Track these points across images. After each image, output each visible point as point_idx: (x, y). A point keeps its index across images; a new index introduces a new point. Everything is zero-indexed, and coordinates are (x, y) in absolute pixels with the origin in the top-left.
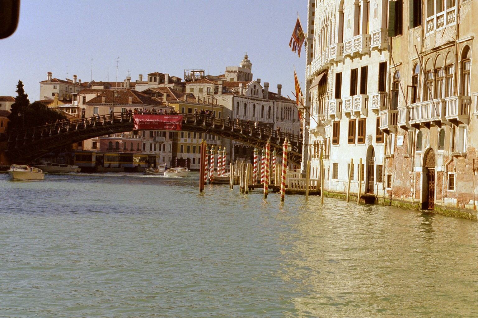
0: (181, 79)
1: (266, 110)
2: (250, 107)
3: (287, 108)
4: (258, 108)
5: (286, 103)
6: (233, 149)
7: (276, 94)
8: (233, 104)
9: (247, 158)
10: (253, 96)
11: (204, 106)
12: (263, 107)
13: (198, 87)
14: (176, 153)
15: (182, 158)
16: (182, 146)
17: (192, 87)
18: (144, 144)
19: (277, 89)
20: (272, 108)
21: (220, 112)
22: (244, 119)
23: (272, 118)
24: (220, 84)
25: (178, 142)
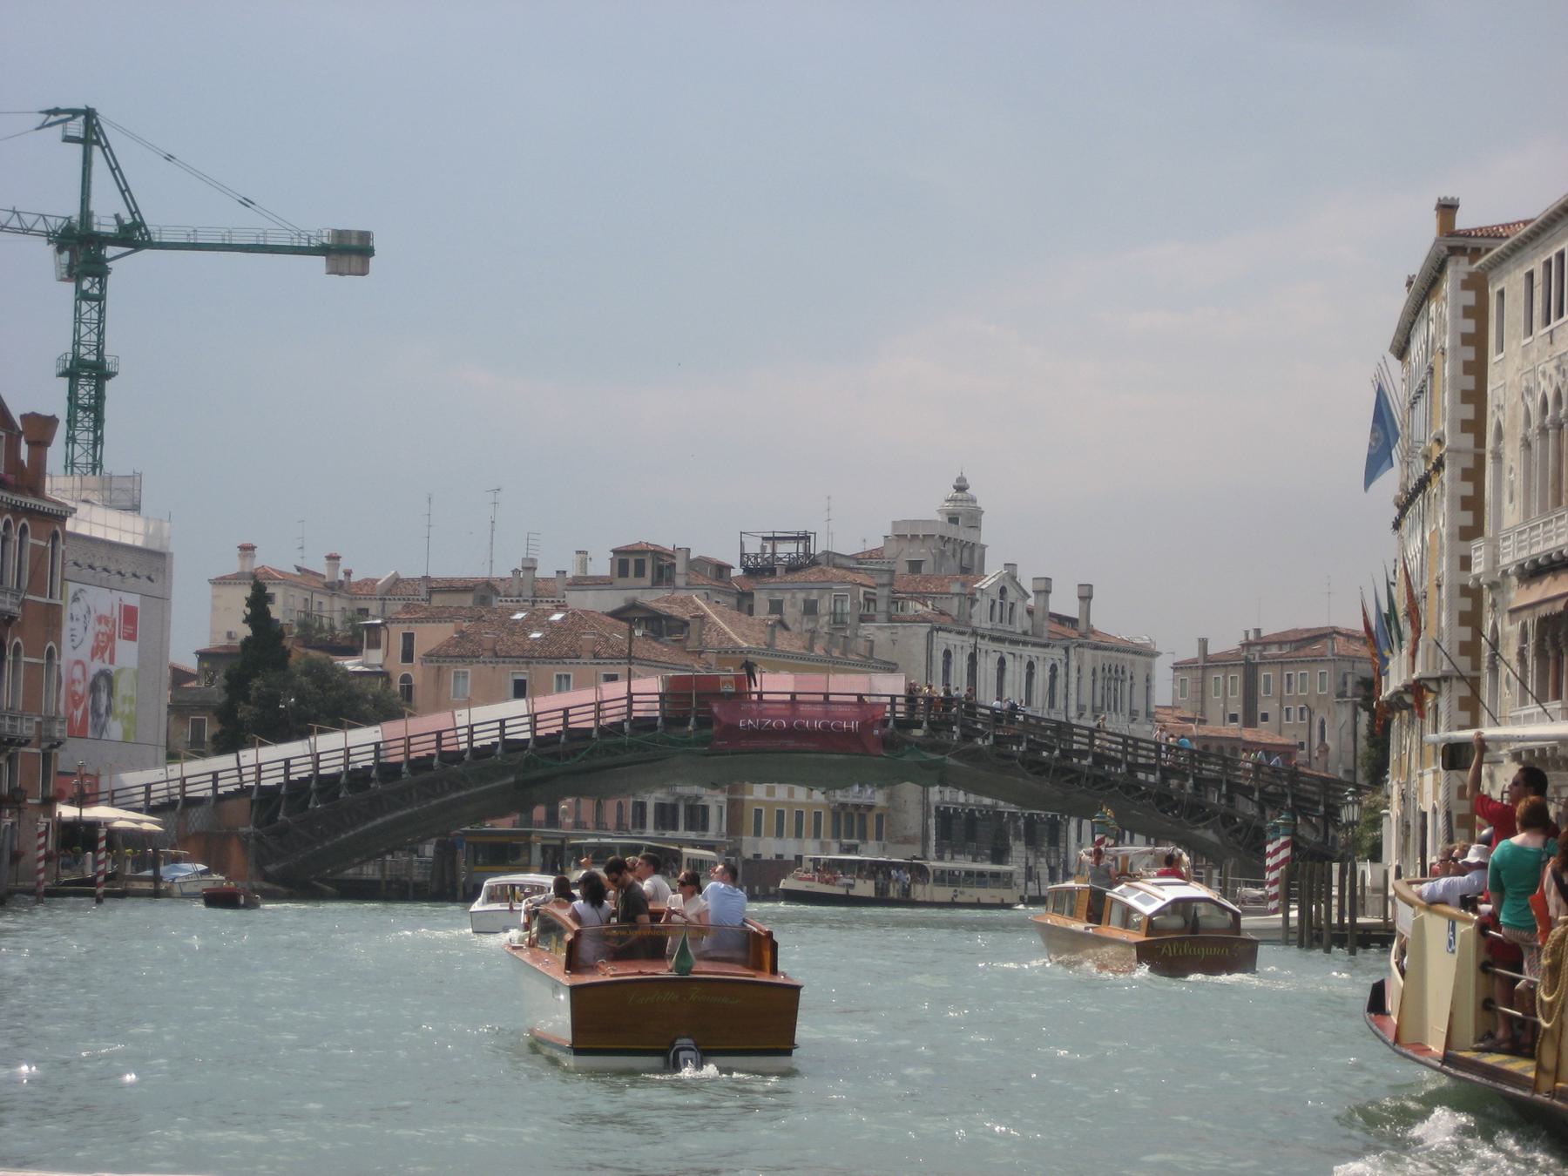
0: (729, 568)
1: (1041, 677)
3: (1110, 670)
4: (1016, 673)
6: (932, 822)
7: (1073, 622)
10: (999, 627)
12: (1031, 666)
13: (801, 596)
15: (757, 856)
16: (758, 812)
17: (778, 596)
20: (1061, 671)
23: (1062, 707)
25: (748, 797)
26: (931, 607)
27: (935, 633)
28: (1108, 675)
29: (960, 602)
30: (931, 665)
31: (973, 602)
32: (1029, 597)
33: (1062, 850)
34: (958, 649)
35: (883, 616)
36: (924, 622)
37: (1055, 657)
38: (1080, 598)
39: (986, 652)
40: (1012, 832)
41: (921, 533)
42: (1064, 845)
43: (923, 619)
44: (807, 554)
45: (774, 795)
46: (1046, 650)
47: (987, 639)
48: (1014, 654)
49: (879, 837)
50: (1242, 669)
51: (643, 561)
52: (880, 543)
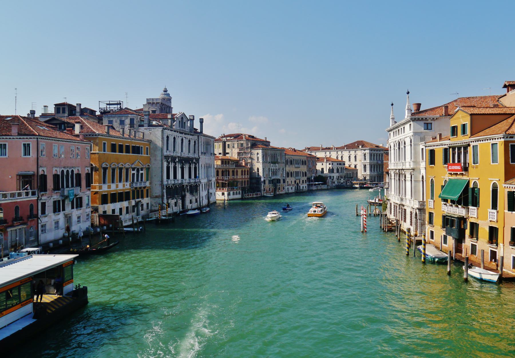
0: (95, 111)
1: (192, 144)
4: (186, 142)
5: (206, 138)
6: (165, 191)
8: (163, 138)
11: (130, 140)
12: (189, 141)
15: (105, 212)
18: (44, 204)
19: (199, 123)
21: (147, 148)
22: (174, 154)
33: (198, 193)
34: (171, 136)
35: (147, 125)
40: (186, 190)
41: (155, 102)
44: (121, 109)
45: (110, 188)
46: (194, 136)
48: (185, 138)
49: (147, 197)
52: (142, 107)
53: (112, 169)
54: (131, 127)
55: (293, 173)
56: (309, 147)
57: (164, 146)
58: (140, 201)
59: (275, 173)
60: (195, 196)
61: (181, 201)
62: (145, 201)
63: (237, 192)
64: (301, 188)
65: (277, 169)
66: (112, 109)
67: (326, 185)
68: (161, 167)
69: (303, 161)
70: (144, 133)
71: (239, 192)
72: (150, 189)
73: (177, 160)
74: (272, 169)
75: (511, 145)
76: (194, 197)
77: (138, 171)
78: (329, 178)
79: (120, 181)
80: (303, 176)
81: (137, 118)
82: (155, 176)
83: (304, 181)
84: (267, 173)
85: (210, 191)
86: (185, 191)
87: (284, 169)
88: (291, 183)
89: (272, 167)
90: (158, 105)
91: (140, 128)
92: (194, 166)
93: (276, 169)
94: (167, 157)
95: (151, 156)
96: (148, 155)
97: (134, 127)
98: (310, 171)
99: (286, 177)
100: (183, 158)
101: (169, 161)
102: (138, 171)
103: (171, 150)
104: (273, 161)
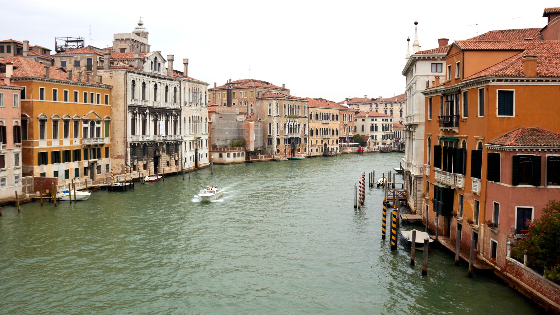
0: (49, 51)
1: (171, 92)
2: (150, 88)
3: (194, 89)
4: (161, 90)
5: (193, 84)
6: (129, 149)
8: (126, 83)
9: (148, 160)
10: (155, 72)
11: (80, 86)
12: (167, 87)
13: (73, 60)
14: (31, 166)
15: (43, 174)
17: (64, 59)
20: (178, 89)
21: (107, 96)
22: (143, 104)
23: (179, 102)
24: (106, 59)
25: (35, 147)
26: (127, 64)
27: (128, 73)
28: (194, 91)
29: (138, 61)
30: (127, 86)
31: (144, 62)
32: (166, 61)
33: (180, 154)
34: (138, 80)
35: (107, 67)
36: (123, 69)
37: (176, 84)
38: (184, 63)
39: (150, 82)
40: (161, 150)
41: (125, 38)
42: (180, 152)
43: (123, 68)
46: (173, 82)
47: (150, 77)
48: (160, 83)
50: (227, 91)
51: (10, 46)
53: (53, 121)
54: (88, 70)
55: (319, 131)
56: (351, 98)
57: (128, 94)
58: (96, 162)
59: (292, 129)
60: (175, 157)
61: (153, 163)
62: (103, 162)
63: (239, 154)
64: (330, 150)
65: (296, 126)
66: (71, 47)
67: (366, 146)
68: (124, 119)
69: (333, 116)
70: (101, 77)
71: (243, 153)
72: (111, 147)
73: (148, 111)
74: (290, 125)
75: (499, 91)
76: (173, 158)
77: (92, 124)
78: (370, 138)
79: (66, 136)
80: (333, 134)
81: (95, 58)
82: (117, 131)
83: (335, 142)
84: (283, 129)
85: (199, 152)
86: (159, 151)
87: (307, 125)
88: (316, 144)
89: (289, 122)
90: (128, 42)
91: (98, 70)
92: (173, 119)
93: (295, 125)
94: (132, 108)
95: (112, 107)
96: (108, 105)
97: (91, 70)
98: (346, 129)
99: (308, 135)
100: (155, 108)
101: (135, 112)
102: (92, 124)
103: (138, 99)
104: (291, 114)
